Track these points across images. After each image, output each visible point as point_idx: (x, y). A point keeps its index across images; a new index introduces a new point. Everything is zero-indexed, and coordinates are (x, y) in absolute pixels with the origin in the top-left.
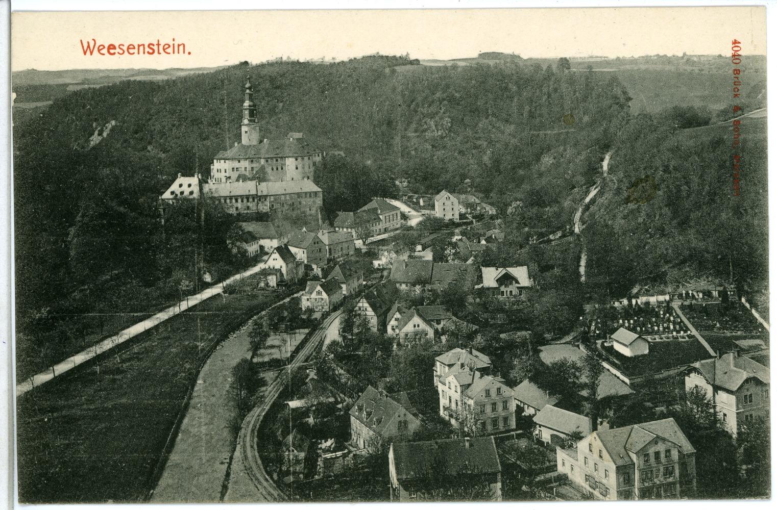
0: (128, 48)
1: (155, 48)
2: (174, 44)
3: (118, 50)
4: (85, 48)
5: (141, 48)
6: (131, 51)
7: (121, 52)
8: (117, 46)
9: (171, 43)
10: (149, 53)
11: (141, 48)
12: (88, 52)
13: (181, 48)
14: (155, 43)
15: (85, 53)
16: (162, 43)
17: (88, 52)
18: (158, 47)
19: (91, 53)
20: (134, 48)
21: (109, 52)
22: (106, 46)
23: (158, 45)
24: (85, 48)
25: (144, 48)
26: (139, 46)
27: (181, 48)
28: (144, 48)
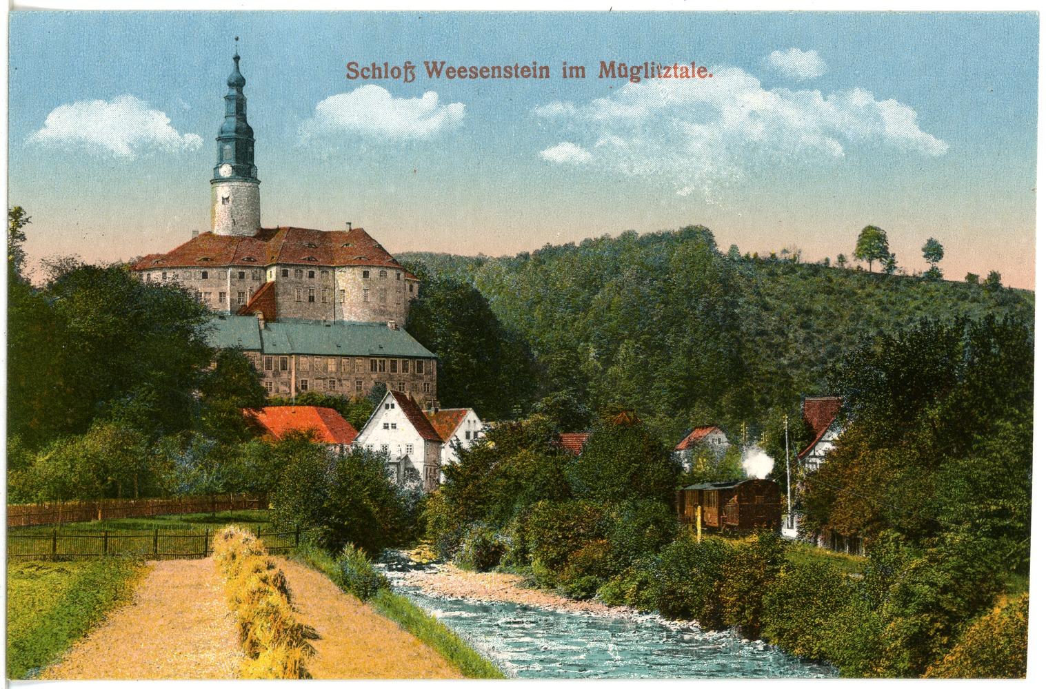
0: (481, 71)
1: (513, 72)
2: (535, 69)
3: (469, 73)
4: (431, 68)
5: (496, 70)
6: (485, 74)
7: (473, 75)
8: (468, 69)
9: (531, 66)
10: (505, 77)
11: (496, 70)
12: (435, 73)
13: (544, 71)
14: (513, 65)
15: (430, 76)
16: (521, 66)
17: (435, 73)
18: (516, 72)
19: (439, 74)
20: (488, 71)
21: (460, 76)
22: (457, 69)
23: (516, 68)
24: (431, 66)
25: (500, 71)
26: (493, 68)
27: (544, 71)
28: (500, 71)
